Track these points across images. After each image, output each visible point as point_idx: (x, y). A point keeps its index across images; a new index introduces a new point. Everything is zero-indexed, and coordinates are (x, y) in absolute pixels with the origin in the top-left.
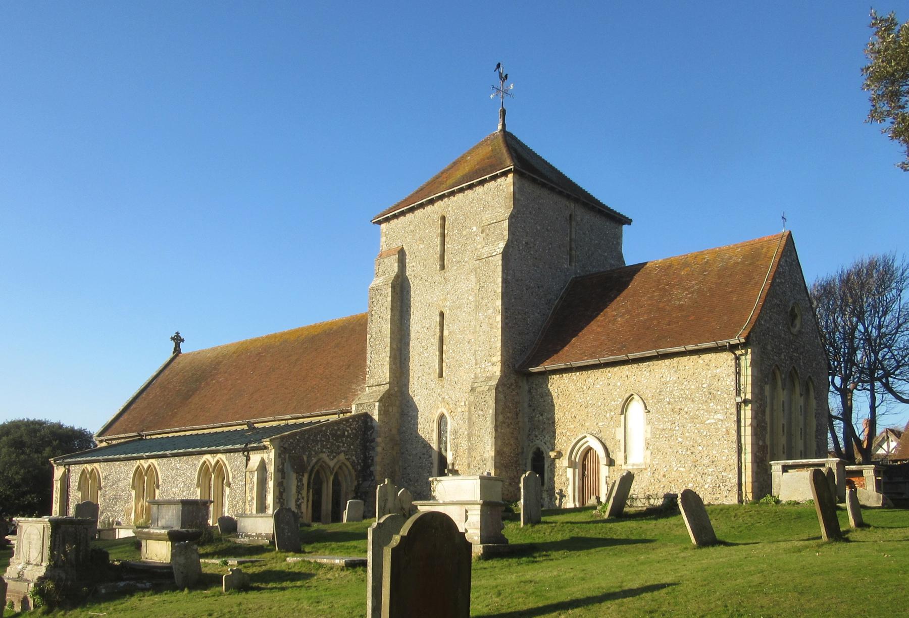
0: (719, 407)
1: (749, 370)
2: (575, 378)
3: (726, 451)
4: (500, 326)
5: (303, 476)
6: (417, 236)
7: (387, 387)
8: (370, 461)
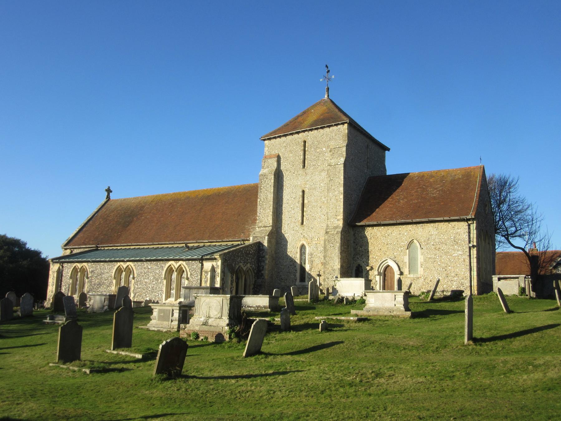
0: (459, 248)
1: (475, 231)
2: (380, 229)
3: (464, 270)
4: (342, 200)
5: (233, 275)
6: (288, 149)
7: (271, 228)
8: (261, 268)
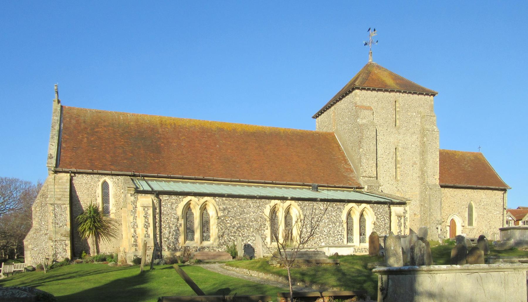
4: (438, 163)
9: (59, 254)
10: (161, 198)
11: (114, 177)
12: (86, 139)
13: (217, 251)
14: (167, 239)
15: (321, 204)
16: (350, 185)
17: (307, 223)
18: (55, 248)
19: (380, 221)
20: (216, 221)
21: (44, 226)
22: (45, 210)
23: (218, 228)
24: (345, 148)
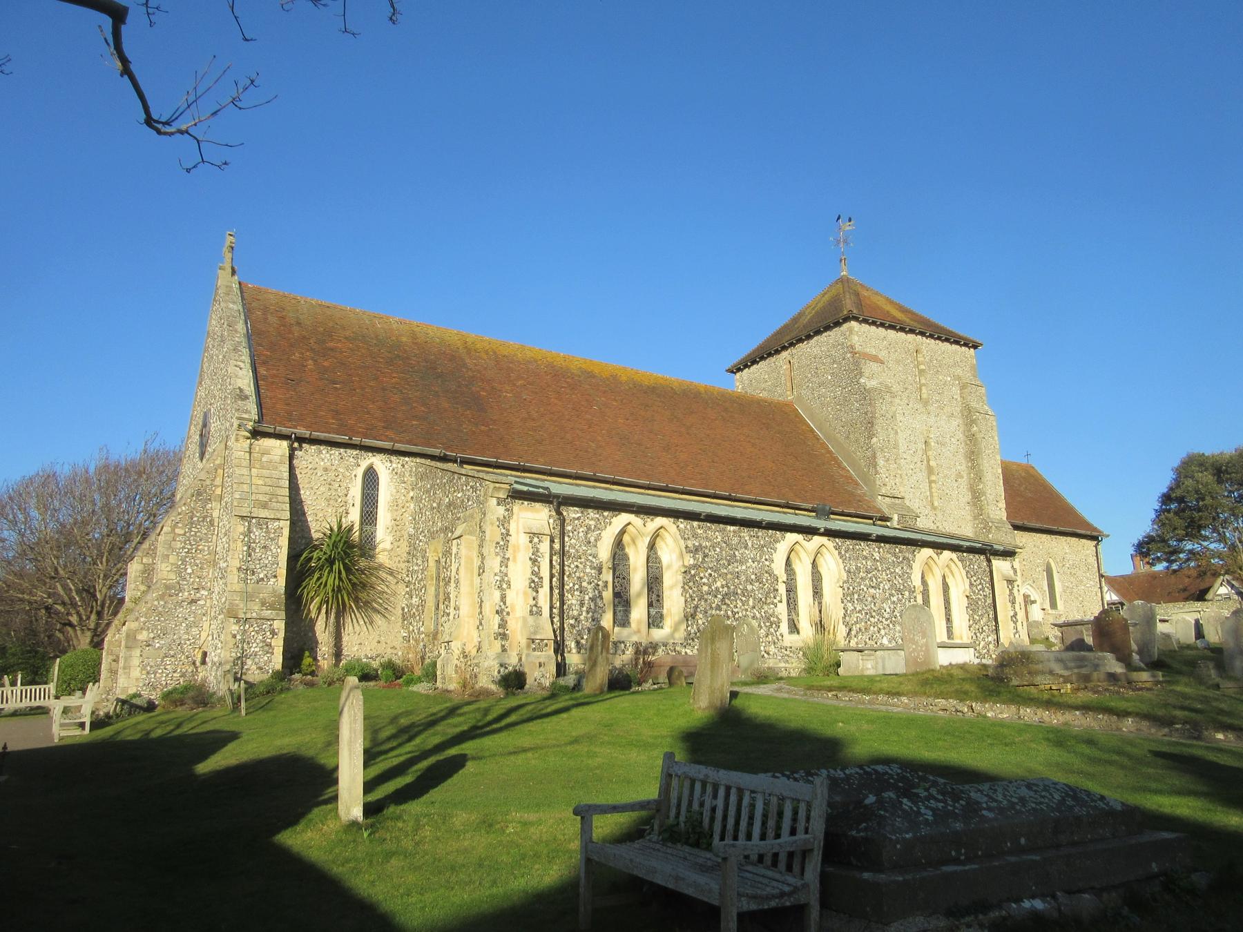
9: (251, 657)
10: (565, 513)
11: (394, 458)
12: (310, 362)
13: (683, 653)
14: (576, 620)
15: (874, 546)
16: (866, 511)
17: (853, 589)
18: (243, 641)
19: (977, 591)
20: (680, 578)
21: (190, 577)
22: (198, 534)
23: (684, 594)
24: (824, 436)
